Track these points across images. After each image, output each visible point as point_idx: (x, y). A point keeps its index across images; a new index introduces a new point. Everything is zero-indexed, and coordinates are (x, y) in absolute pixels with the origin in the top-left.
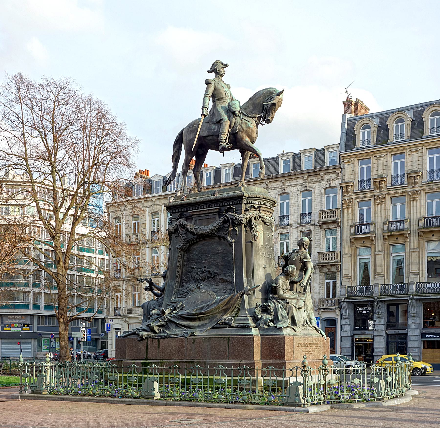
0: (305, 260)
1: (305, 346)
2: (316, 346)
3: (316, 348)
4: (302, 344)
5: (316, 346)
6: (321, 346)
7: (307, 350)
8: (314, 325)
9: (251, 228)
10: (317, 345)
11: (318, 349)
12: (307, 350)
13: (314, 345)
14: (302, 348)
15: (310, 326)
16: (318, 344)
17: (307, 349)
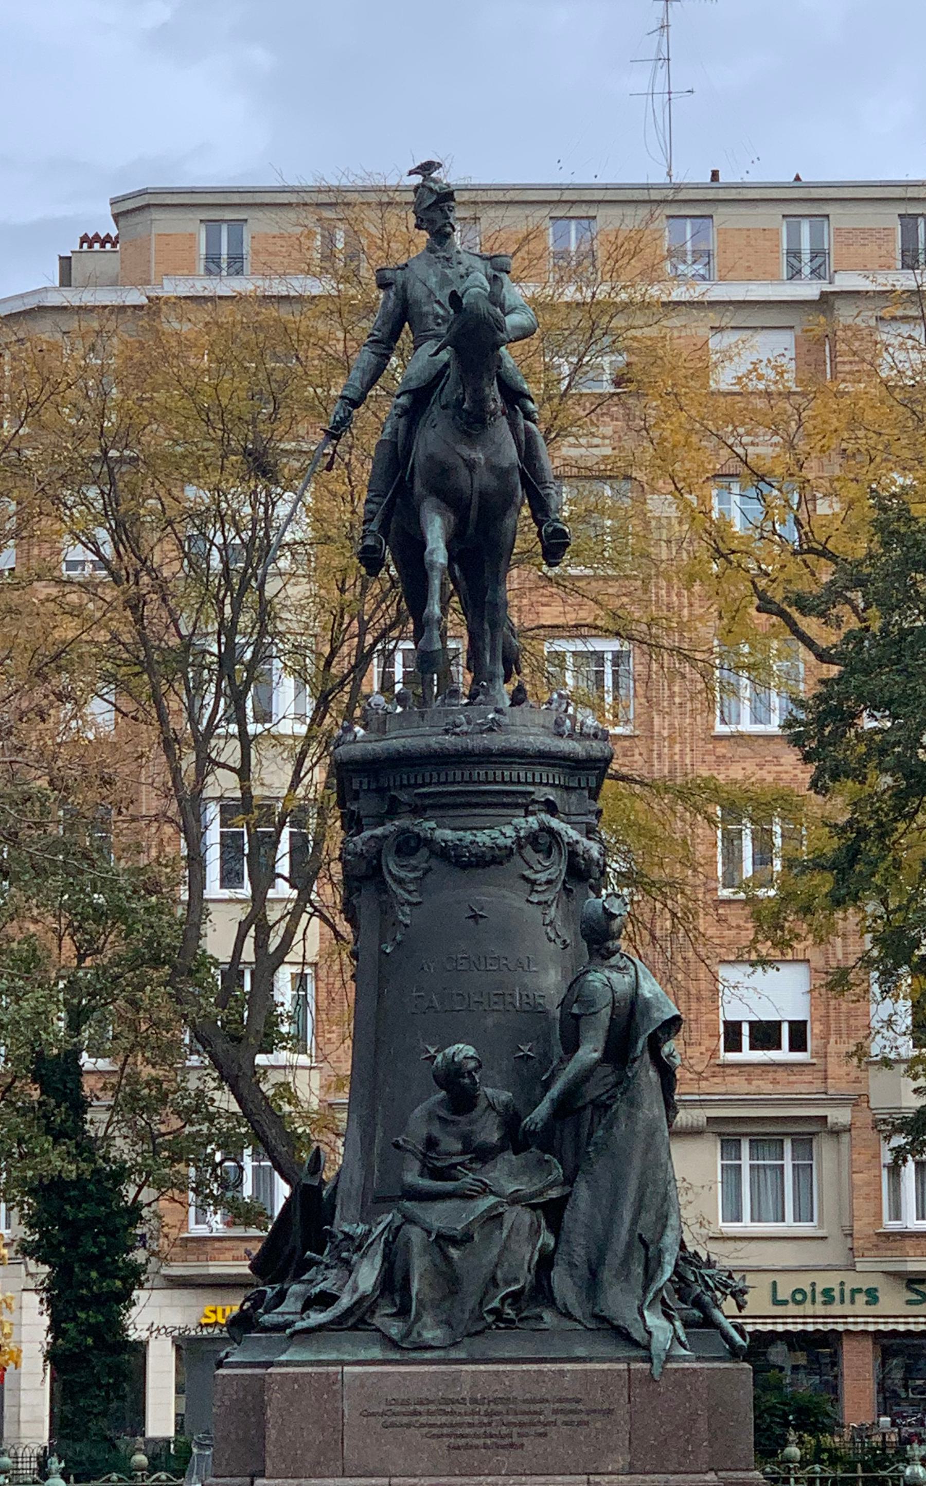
0: (575, 1010)
1: (453, 1413)
2: (555, 1412)
3: (561, 1418)
4: (421, 1403)
5: (555, 1412)
6: (610, 1412)
7: (468, 1431)
8: (597, 1310)
9: (383, 887)
10: (574, 1406)
11: (587, 1423)
12: (468, 1431)
13: (537, 1407)
14: (423, 1419)
15: (568, 1315)
16: (578, 1401)
17: (471, 1425)
